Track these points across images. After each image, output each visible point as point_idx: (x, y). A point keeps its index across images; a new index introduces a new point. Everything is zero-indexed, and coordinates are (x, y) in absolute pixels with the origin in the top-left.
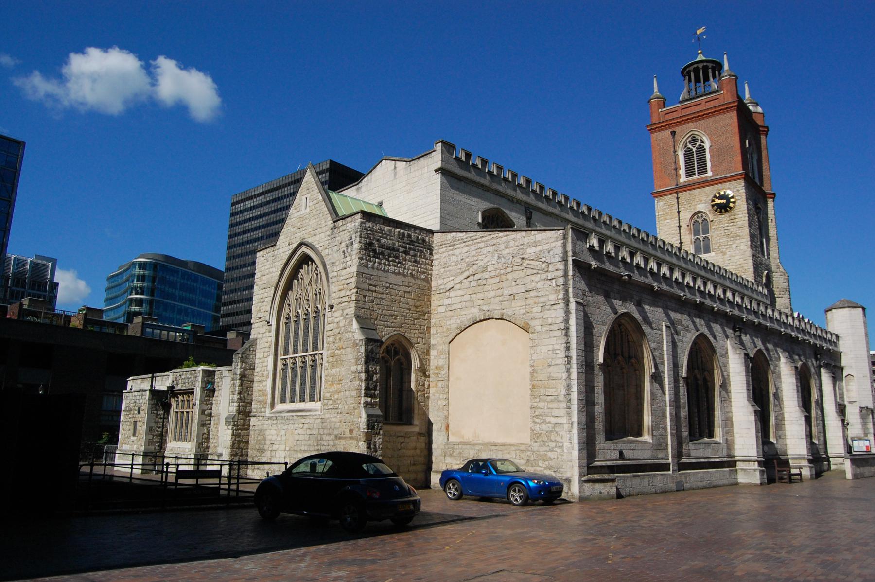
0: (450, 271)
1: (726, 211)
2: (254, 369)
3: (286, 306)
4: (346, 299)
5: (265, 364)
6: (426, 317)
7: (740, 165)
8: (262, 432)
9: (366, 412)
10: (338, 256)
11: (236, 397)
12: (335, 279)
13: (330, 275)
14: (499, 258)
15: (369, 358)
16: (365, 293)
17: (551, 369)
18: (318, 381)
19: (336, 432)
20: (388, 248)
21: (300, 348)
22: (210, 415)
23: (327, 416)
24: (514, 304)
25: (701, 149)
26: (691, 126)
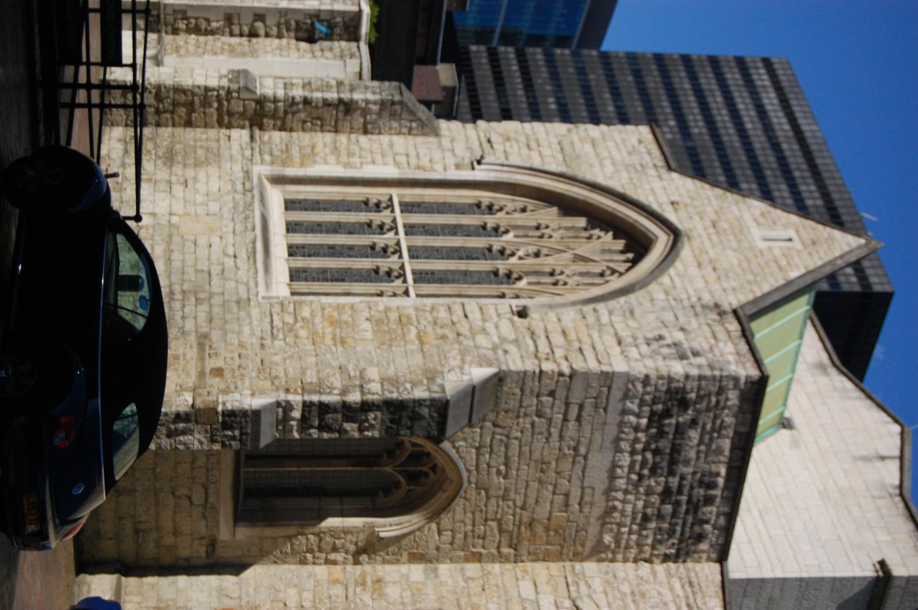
2: (366, 132)
3: (520, 202)
4: (543, 348)
5: (378, 158)
6: (505, 550)
8: (214, 157)
9: (266, 408)
10: (649, 325)
11: (298, 93)
12: (591, 319)
13: (602, 307)
15: (398, 411)
16: (561, 393)
19: (215, 336)
20: (676, 449)
21: (420, 241)
22: (253, 34)
23: (255, 312)
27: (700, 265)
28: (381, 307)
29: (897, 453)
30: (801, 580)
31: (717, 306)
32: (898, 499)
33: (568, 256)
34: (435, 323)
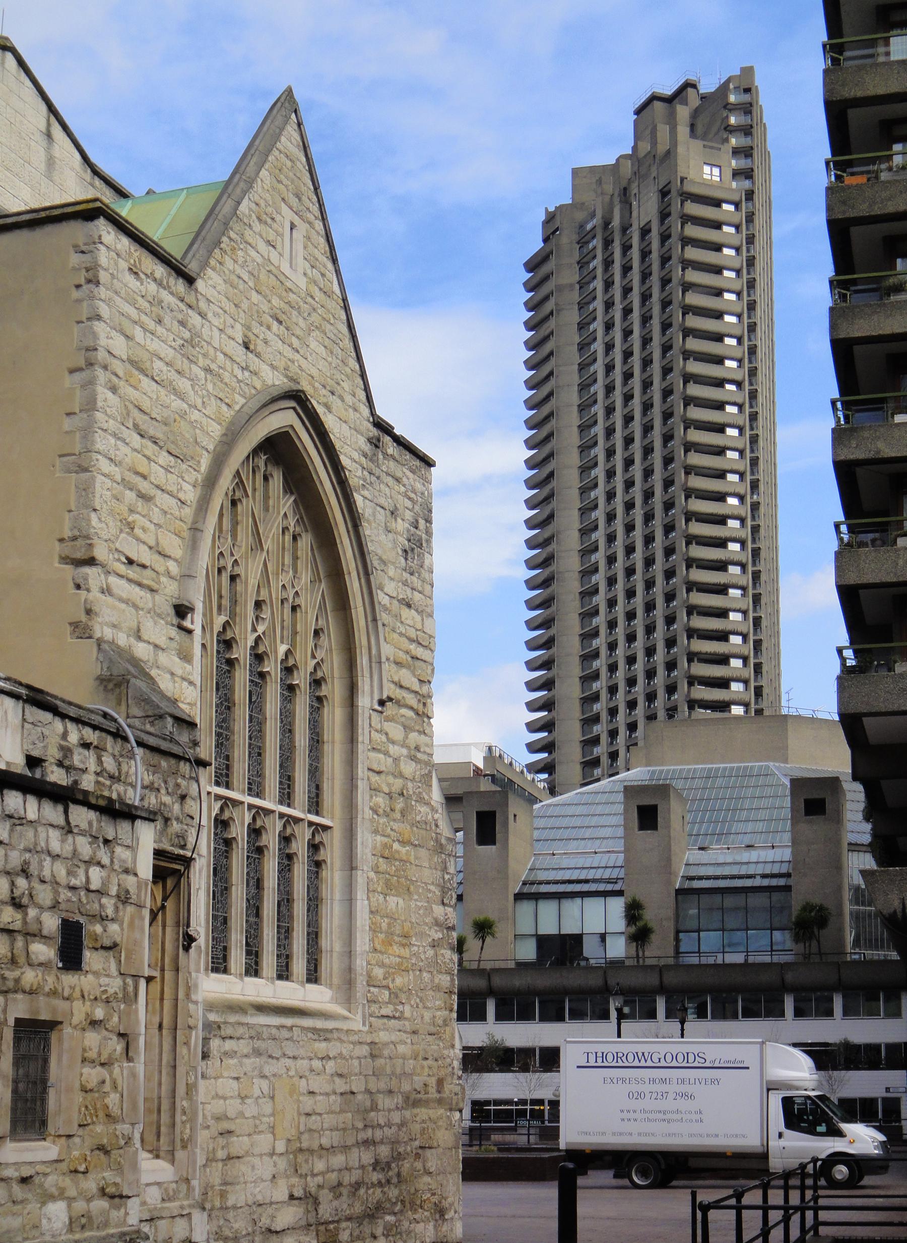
19: (406, 1087)
23: (383, 1037)
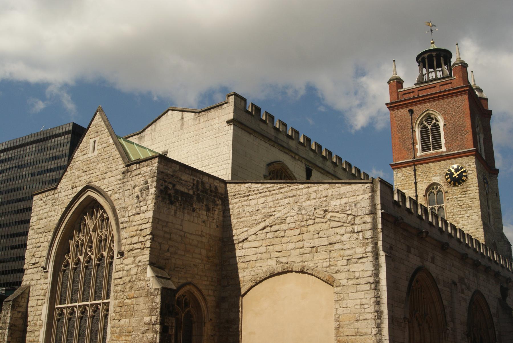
0: (244, 221)
1: (459, 184)
5: (38, 313)
7: (471, 143)
10: (131, 202)
12: (125, 225)
13: (121, 220)
14: (300, 210)
17: (359, 324)
18: (100, 333)
21: (79, 296)
24: (316, 256)
25: (436, 127)
26: (427, 106)
27: (104, 179)
28: (114, 314)
29: (181, 113)
30: (233, 153)
31: (123, 173)
32: (200, 114)
33: (93, 234)
34: (123, 291)
